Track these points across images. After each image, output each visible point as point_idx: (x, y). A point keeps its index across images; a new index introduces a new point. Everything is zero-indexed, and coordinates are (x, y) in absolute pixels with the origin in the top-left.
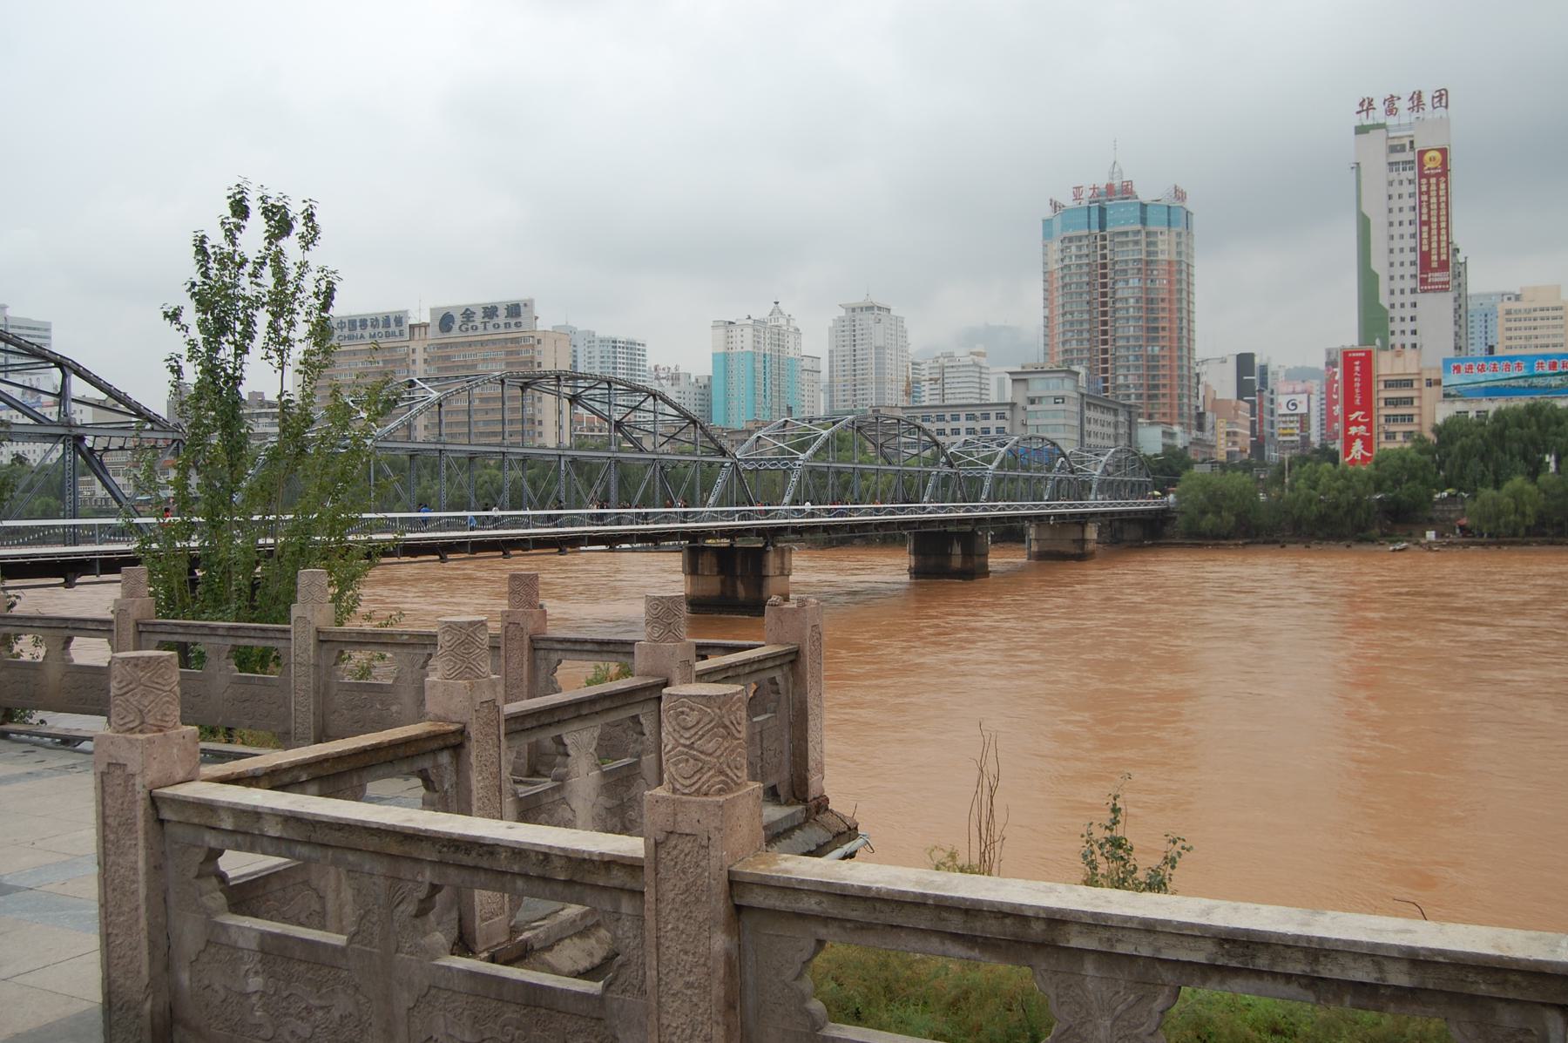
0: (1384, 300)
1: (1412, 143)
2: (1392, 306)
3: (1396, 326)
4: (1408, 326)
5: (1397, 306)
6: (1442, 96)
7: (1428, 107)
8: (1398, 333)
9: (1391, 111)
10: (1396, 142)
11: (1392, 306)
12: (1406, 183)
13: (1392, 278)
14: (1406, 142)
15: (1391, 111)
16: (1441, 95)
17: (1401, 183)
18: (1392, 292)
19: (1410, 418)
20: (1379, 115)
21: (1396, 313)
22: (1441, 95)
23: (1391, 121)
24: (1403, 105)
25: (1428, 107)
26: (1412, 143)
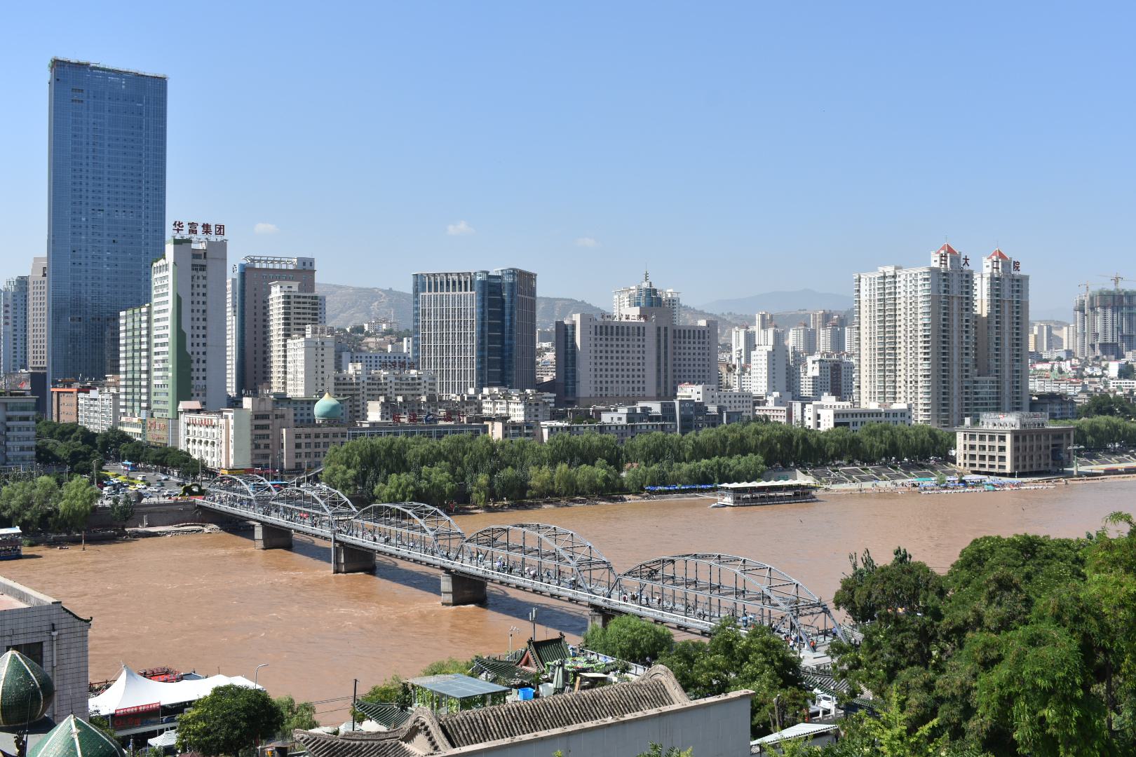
0: (189, 349)
1: (205, 253)
2: (192, 353)
3: (194, 366)
4: (202, 366)
5: (195, 353)
6: (220, 229)
7: (213, 233)
8: (195, 370)
9: (193, 231)
10: (196, 252)
11: (192, 353)
12: (201, 278)
13: (192, 336)
14: (202, 253)
15: (193, 231)
16: (220, 229)
17: (198, 278)
18: (192, 345)
19: (268, 436)
20: (185, 234)
21: (194, 358)
22: (220, 229)
23: (194, 237)
24: (200, 229)
25: (213, 233)
26: (205, 253)
